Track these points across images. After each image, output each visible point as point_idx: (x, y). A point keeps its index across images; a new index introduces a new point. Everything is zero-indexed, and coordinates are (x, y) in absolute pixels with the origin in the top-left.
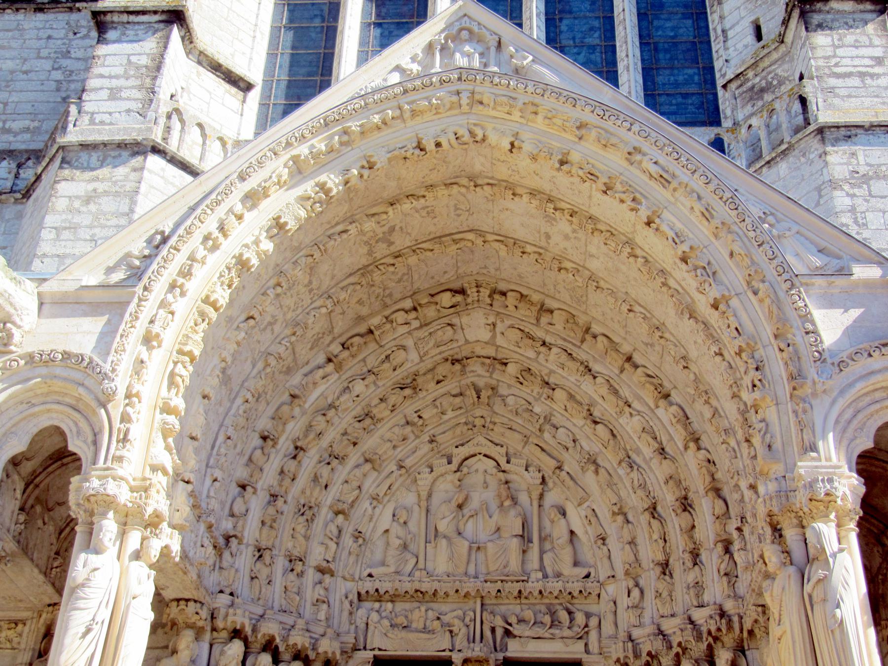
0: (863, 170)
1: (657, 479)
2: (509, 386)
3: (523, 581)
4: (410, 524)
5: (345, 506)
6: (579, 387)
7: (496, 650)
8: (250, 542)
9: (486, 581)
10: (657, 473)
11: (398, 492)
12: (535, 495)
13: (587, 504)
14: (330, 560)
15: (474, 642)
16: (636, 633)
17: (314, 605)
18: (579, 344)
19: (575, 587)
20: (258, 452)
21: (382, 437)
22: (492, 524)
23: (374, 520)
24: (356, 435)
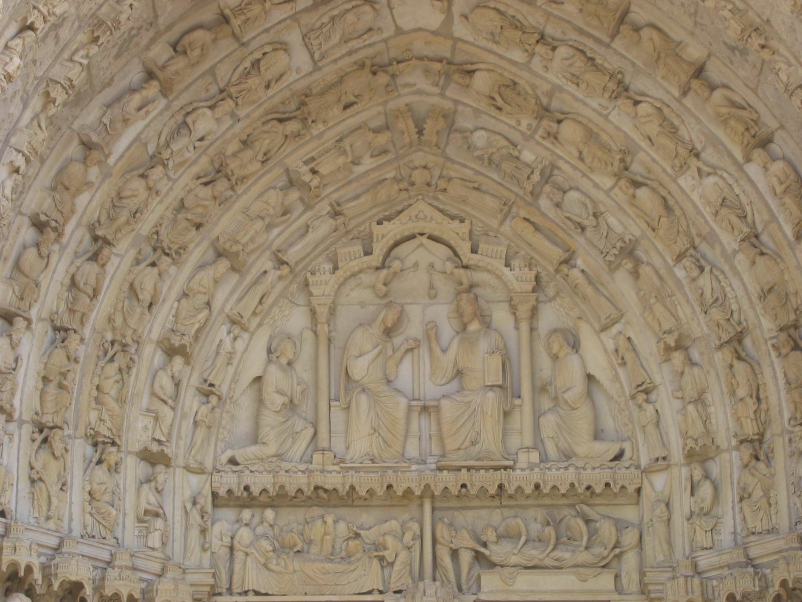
1: (746, 289)
2: (477, 112)
3: (506, 468)
4: (298, 366)
5: (186, 340)
6: (606, 117)
7: (460, 589)
8: (25, 417)
9: (440, 469)
10: (746, 279)
11: (276, 310)
12: (524, 311)
13: (617, 327)
14: (163, 439)
15: (421, 577)
16: (705, 560)
17: (140, 521)
18: (607, 40)
19: (596, 478)
20: (32, 253)
21: (245, 211)
22: (447, 361)
23: (235, 362)
24: (200, 210)
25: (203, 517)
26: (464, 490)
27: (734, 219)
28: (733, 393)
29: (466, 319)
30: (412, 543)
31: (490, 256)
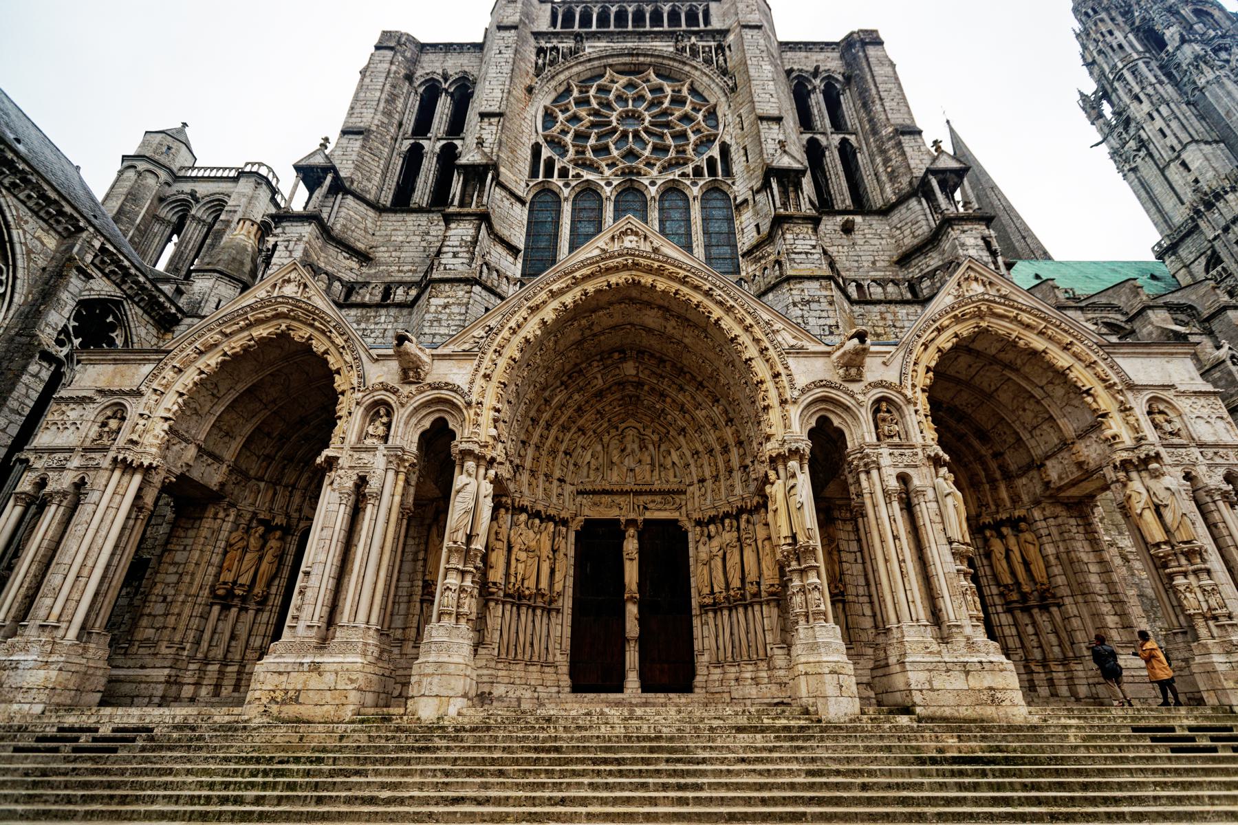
0: (807, 298)
19: (675, 487)
31: (648, 432)
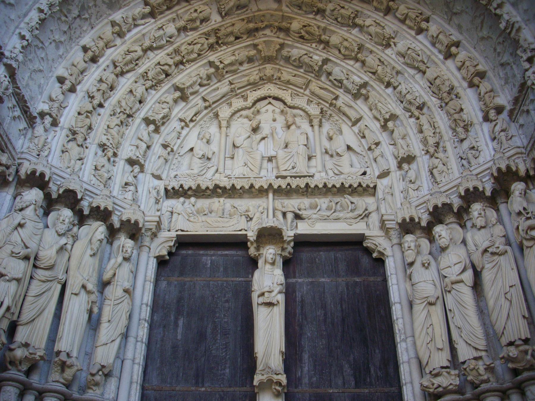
9: (277, 177)
10: (421, 83)
11: (202, 122)
12: (316, 122)
23: (181, 138)
25: (158, 196)
26: (289, 187)
27: (414, 55)
28: (421, 132)
29: (289, 123)
30: (262, 211)
